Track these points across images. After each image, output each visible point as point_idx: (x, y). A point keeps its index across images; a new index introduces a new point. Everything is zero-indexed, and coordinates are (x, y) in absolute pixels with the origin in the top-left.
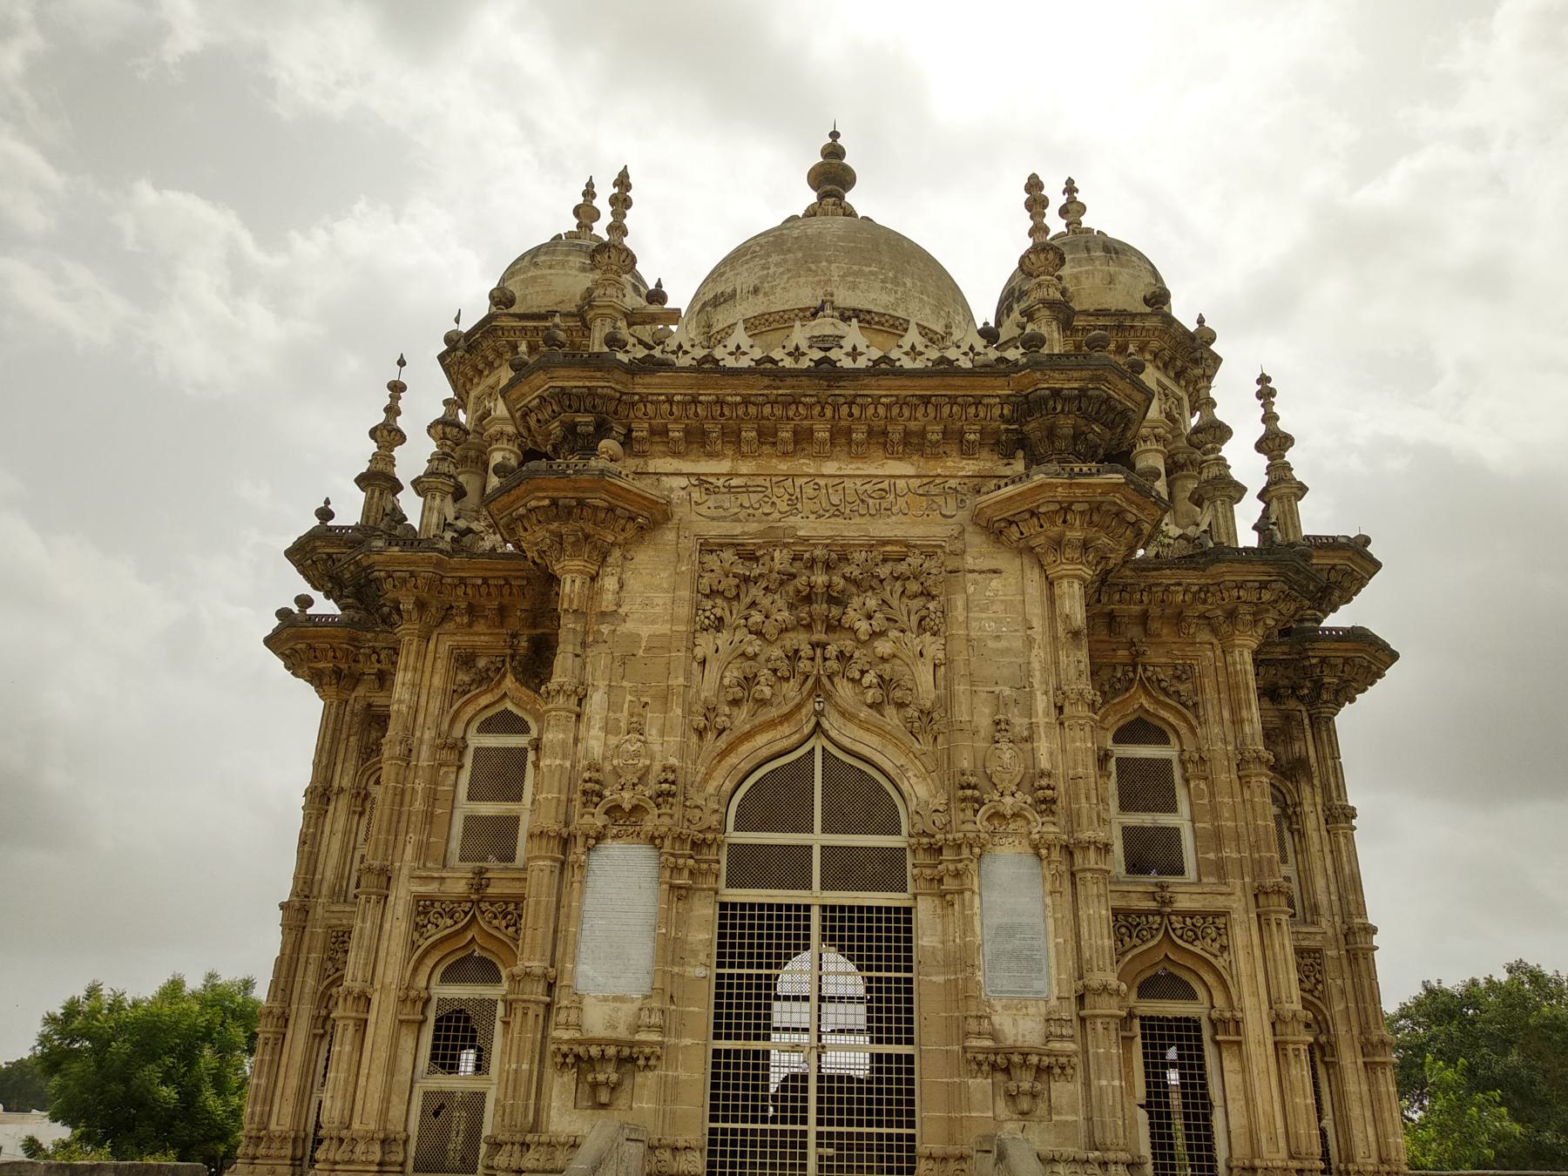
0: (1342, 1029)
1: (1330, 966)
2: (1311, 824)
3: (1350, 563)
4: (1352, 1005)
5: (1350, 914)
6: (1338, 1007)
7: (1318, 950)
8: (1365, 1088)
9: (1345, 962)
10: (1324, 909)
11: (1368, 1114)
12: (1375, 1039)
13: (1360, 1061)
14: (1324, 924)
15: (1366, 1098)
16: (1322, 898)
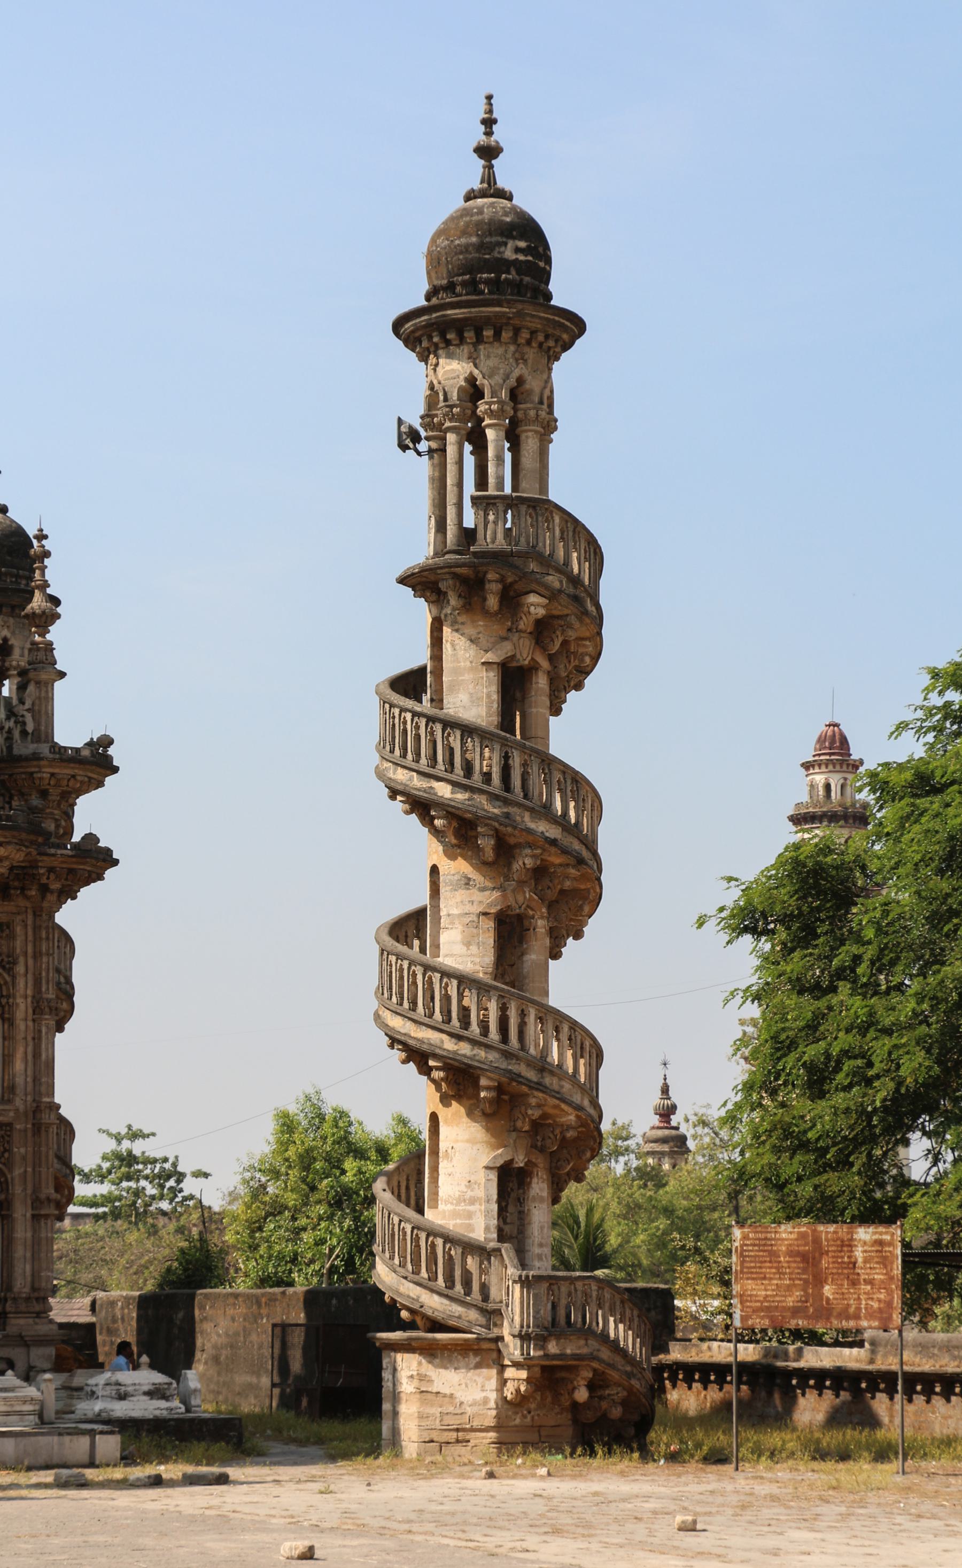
0: (18, 1190)
1: (16, 1137)
2: (20, 1014)
3: (96, 763)
4: (29, 1170)
5: (40, 1094)
6: (17, 1172)
7: (10, 1125)
8: (29, 1235)
9: (30, 1134)
10: (19, 1091)
11: (29, 1255)
12: (43, 1196)
13: (29, 1215)
14: (19, 1103)
15: (29, 1242)
16: (20, 1080)
